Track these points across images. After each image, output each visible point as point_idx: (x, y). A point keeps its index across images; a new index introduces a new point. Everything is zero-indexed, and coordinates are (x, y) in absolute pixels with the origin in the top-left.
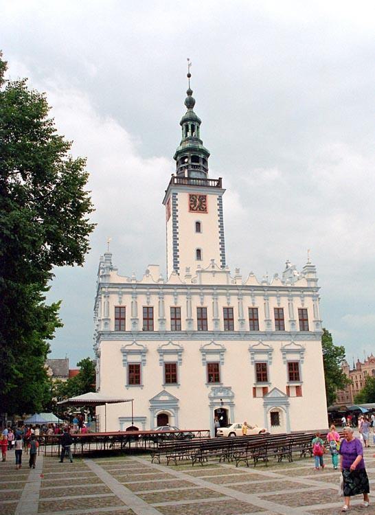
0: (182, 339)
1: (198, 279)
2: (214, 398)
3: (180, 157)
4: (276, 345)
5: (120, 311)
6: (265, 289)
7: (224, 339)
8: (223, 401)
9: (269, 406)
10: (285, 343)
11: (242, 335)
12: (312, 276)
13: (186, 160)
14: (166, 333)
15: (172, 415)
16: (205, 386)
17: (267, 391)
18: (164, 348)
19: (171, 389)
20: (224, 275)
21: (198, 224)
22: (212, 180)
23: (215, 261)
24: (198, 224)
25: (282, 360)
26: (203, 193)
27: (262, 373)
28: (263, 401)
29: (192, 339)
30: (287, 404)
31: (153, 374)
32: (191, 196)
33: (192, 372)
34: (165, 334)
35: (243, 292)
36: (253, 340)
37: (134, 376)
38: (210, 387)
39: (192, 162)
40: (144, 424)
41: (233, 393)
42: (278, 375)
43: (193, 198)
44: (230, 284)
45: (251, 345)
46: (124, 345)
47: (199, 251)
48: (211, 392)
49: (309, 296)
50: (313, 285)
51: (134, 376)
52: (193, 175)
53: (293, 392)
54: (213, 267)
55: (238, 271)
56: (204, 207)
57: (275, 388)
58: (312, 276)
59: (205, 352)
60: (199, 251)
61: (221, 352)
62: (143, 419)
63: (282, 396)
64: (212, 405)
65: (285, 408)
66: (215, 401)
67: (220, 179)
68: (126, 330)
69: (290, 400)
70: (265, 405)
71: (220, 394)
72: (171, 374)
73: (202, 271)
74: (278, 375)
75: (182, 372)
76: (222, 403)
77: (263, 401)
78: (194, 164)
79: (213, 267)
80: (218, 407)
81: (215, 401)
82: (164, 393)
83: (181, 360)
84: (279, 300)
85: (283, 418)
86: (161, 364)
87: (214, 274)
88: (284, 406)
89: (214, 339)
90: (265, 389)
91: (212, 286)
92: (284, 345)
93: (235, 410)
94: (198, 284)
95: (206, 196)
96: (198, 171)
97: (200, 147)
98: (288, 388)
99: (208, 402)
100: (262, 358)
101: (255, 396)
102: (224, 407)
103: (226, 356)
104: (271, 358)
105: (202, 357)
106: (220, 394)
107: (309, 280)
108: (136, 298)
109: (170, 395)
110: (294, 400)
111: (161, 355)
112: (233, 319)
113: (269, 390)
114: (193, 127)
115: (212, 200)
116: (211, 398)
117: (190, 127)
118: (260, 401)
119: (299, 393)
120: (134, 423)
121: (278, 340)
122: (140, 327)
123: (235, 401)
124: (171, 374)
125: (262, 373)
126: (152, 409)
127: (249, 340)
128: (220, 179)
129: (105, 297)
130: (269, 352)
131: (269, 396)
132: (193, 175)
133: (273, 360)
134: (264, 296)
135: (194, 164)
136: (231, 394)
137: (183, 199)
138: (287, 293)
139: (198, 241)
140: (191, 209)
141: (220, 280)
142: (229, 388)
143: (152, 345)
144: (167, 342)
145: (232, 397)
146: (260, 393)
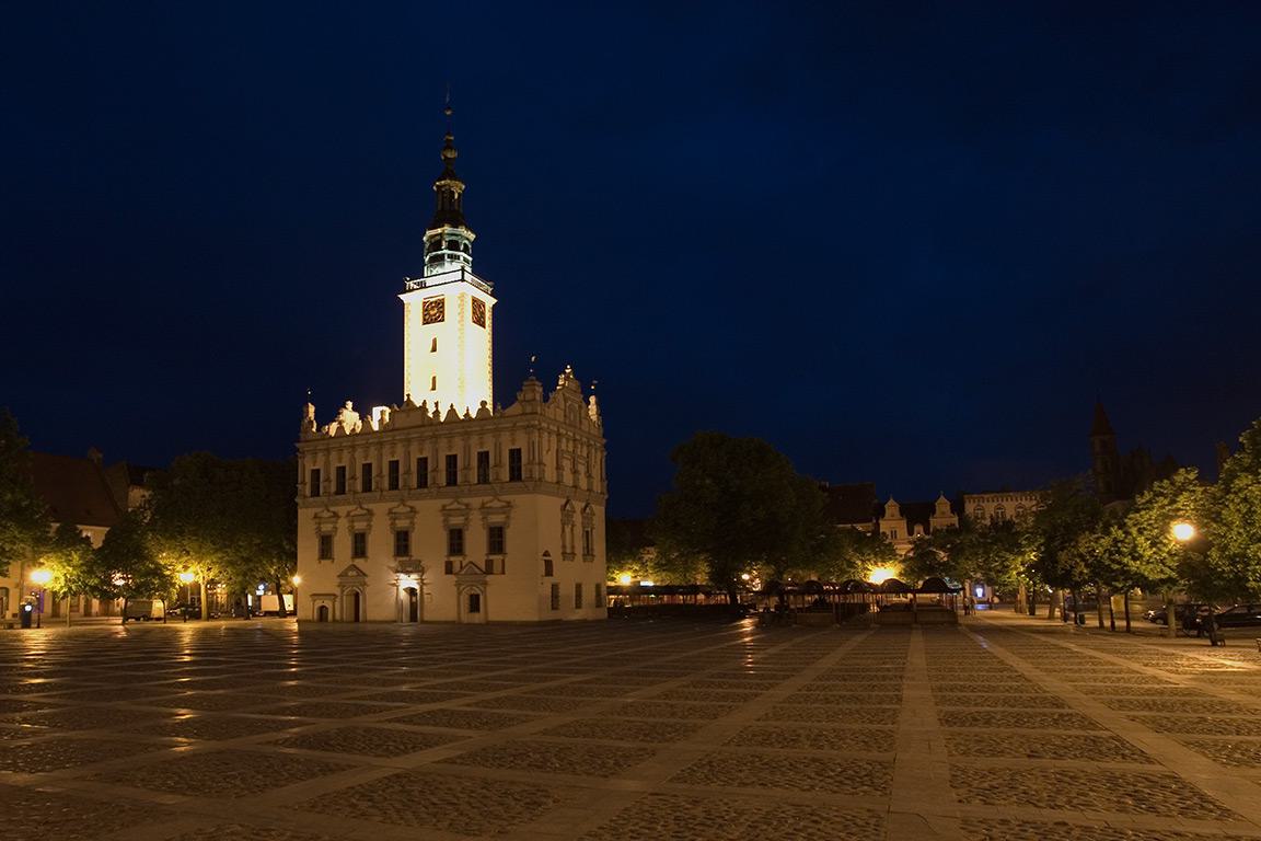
4: (476, 502)
19: (359, 562)
57: (471, 562)
69: (489, 578)
70: (458, 584)
100: (456, 521)
122: (333, 489)
126: (341, 585)
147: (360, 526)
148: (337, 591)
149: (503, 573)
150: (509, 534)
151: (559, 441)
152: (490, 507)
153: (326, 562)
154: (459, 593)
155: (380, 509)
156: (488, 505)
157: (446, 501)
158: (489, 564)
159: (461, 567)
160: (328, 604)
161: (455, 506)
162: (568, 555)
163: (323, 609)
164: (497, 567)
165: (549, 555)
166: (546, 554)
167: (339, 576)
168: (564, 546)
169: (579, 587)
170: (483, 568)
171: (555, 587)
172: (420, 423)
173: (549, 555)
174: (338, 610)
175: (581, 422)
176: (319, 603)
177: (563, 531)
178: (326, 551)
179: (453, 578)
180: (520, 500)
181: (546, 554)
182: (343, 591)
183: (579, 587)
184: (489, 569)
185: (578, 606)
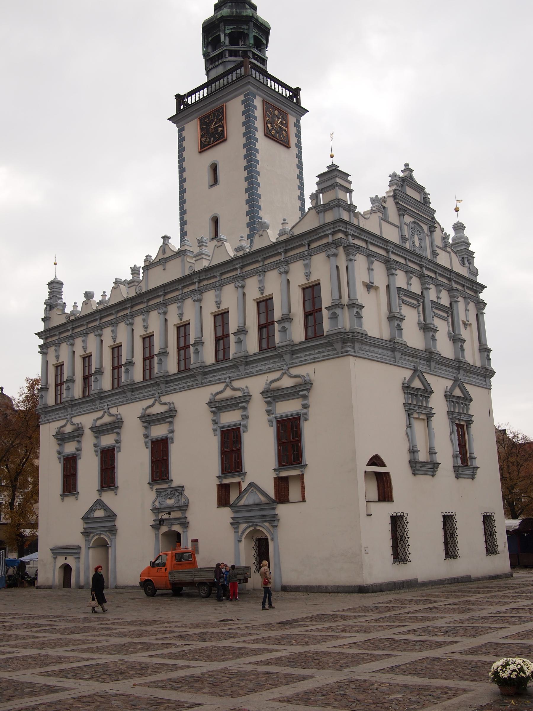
0: (122, 403)
4: (255, 385)
7: (175, 391)
8: (173, 515)
9: (243, 526)
18: (99, 423)
19: (108, 498)
20: (178, 261)
21: (214, 168)
24: (214, 168)
25: (266, 417)
30: (274, 520)
33: (134, 462)
38: (156, 487)
44: (187, 273)
47: (215, 221)
59: (148, 420)
62: (74, 551)
63: (263, 499)
69: (282, 510)
70: (235, 524)
78: (234, 48)
80: (164, 529)
82: (99, 504)
87: (164, 265)
88: (267, 524)
89: (160, 395)
94: (144, 290)
99: (150, 518)
100: (230, 418)
105: (142, 431)
109: (105, 508)
116: (155, 510)
121: (260, 373)
126: (86, 533)
127: (211, 383)
131: (242, 502)
135: (234, 48)
136: (182, 501)
142: (181, 488)
147: (107, 441)
149: (304, 500)
150: (308, 430)
151: (390, 273)
152: (279, 389)
153: (70, 500)
155: (131, 413)
156: (275, 385)
158: (282, 484)
159: (240, 493)
160: (71, 561)
162: (423, 467)
163: (67, 569)
165: (384, 465)
166: (376, 461)
168: (413, 451)
169: (448, 520)
170: (271, 493)
171: (397, 522)
173: (384, 465)
175: (435, 254)
176: (61, 561)
177: (409, 425)
178: (70, 485)
179: (227, 513)
180: (323, 373)
181: (376, 461)
182: (88, 541)
183: (448, 520)
184: (282, 495)
185: (450, 551)
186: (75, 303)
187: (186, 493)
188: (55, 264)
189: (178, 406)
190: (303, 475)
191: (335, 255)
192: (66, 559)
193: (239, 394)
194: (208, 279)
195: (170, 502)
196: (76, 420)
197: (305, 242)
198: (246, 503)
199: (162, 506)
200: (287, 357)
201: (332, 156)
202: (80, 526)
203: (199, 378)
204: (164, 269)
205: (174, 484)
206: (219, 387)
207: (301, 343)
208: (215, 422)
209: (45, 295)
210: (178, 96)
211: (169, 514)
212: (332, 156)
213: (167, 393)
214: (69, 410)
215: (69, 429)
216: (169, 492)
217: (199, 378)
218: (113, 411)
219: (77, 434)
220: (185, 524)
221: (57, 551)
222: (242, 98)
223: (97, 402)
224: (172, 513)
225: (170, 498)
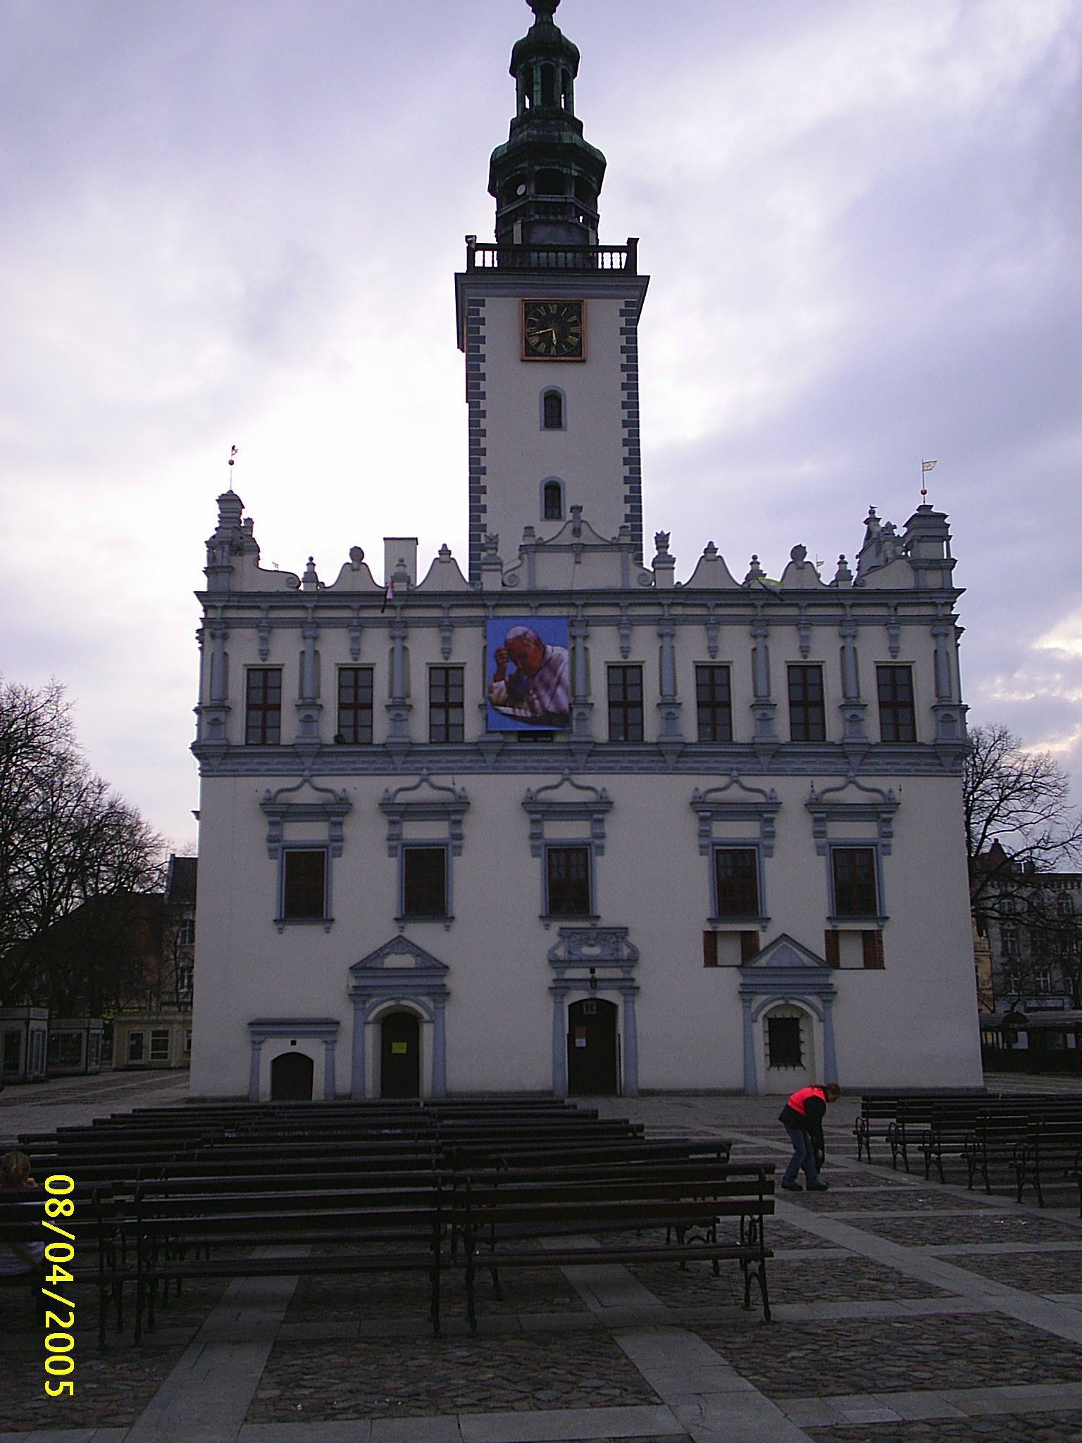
1: (523, 575)
2: (569, 963)
3: (505, 173)
4: (793, 791)
5: (264, 681)
6: (757, 602)
8: (599, 973)
10: (821, 783)
11: (670, 757)
12: (926, 550)
13: (521, 190)
14: (411, 750)
15: (426, 1017)
16: (541, 924)
17: (756, 945)
18: (402, 798)
19: (424, 934)
22: (612, 249)
23: (583, 516)
26: (569, 295)
27: (737, 882)
28: (741, 980)
29: (496, 771)
30: (827, 993)
31: (365, 882)
32: (530, 309)
33: (497, 873)
34: (409, 753)
35: (678, 611)
36: (709, 772)
37: (305, 890)
38: (556, 926)
39: (538, 192)
40: (331, 1044)
41: (634, 950)
42: (796, 895)
43: (538, 315)
44: (634, 585)
45: (702, 790)
46: (274, 790)
48: (555, 948)
49: (919, 620)
50: (932, 580)
51: (305, 890)
52: (542, 235)
53: (851, 952)
54: (577, 532)
55: (662, 540)
56: (573, 340)
58: (926, 550)
60: (552, 492)
61: (598, 810)
62: (326, 1028)
63: (808, 961)
64: (559, 988)
65: (820, 1006)
66: (571, 974)
67: (633, 242)
68: (283, 742)
69: (838, 979)
70: (746, 993)
71: (587, 951)
72: (425, 885)
73: (541, 546)
74: (796, 895)
75: (466, 879)
76: (593, 981)
77: (741, 980)
79: (577, 532)
80: (578, 995)
81: (571, 974)
82: (400, 944)
83: (459, 837)
84: (804, 638)
85: (813, 1037)
86: (392, 851)
87: (577, 555)
89: (574, 771)
90: (749, 943)
91: (570, 593)
92: (818, 790)
93: (640, 1006)
94: (523, 586)
95: (579, 305)
96: (557, 223)
97: (567, 137)
98: (832, 938)
99: (547, 977)
101: (711, 959)
102: (602, 995)
103: (612, 826)
104: (772, 835)
106: (587, 951)
107: (917, 566)
108: (316, 638)
109: (418, 952)
110: (851, 982)
111: (392, 823)
112: (640, 704)
113: (764, 940)
114: (548, 73)
115: (601, 316)
116: (554, 962)
117: (537, 75)
118: (727, 980)
119: (873, 960)
120: (298, 1041)
122: (328, 729)
123: (640, 975)
124: (425, 885)
125: (737, 882)
126: (359, 995)
127: (692, 771)
128: (633, 242)
129: (213, 636)
130: (766, 811)
131: (763, 962)
132: (542, 235)
133: (779, 843)
134: (751, 623)
136: (625, 952)
137: (503, 316)
138: (837, 611)
139: (553, 455)
140: (530, 353)
141: (601, 573)
142: (620, 933)
143: (366, 790)
144: (414, 780)
145: (632, 960)
146: (729, 951)
148: (344, 1013)
154: (750, 1019)
157: (705, 782)
160: (311, 1047)
161: (735, 794)
164: (851, 952)
167: (351, 968)
172: (617, 584)
174: (346, 1066)
176: (276, 1047)
186: (311, 559)
187: (632, 939)
188: (231, 463)
189: (612, 795)
190: (880, 932)
191: (946, 635)
192: (294, 1043)
193: (760, 798)
194: (684, 605)
195: (596, 951)
196: (338, 784)
197: (893, 602)
198: (775, 964)
199: (574, 958)
200: (855, 760)
201: (924, 493)
202: (343, 982)
203: (671, 759)
204: (578, 562)
205: (602, 923)
206: (720, 781)
207: (877, 745)
208: (704, 834)
209: (209, 522)
210: (470, 240)
211: (592, 971)
212: (924, 493)
213: (589, 771)
214: (308, 761)
215: (307, 796)
216: (594, 933)
217: (671, 759)
218: (445, 780)
219: (335, 811)
220: (630, 988)
221: (261, 1028)
222: (621, 304)
223: (398, 760)
224: (597, 970)
225: (592, 946)
